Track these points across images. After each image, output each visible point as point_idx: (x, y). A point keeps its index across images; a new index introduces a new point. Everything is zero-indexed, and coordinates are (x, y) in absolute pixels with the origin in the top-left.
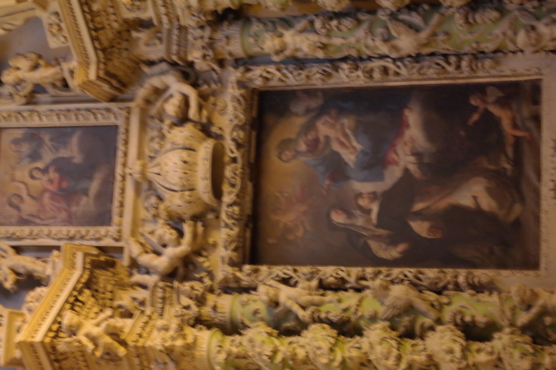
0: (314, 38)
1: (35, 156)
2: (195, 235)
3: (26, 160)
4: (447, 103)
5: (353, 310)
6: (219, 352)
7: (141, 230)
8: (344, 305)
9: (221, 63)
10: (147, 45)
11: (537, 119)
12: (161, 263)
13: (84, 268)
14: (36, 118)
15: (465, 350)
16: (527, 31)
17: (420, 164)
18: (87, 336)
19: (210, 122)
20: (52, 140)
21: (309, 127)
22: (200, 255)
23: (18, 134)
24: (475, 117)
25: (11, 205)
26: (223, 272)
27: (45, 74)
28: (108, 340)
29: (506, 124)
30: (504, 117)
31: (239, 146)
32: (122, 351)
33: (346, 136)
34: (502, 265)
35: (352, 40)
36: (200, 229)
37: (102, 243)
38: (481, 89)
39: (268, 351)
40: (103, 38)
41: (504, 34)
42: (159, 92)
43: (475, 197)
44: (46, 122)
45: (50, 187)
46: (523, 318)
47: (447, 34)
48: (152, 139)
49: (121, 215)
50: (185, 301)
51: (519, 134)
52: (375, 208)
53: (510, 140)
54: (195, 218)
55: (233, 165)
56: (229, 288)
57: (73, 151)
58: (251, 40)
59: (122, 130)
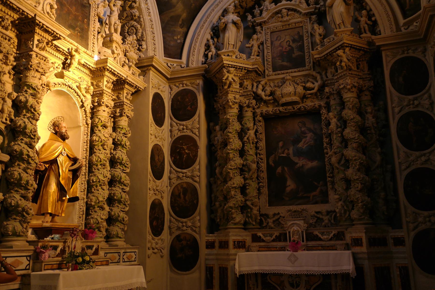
1: (294, 41)
2: (269, 100)
3: (292, 38)
5: (248, 153)
6: (230, 116)
7: (271, 82)
8: (249, 150)
10: (331, 72)
11: (316, 203)
12: (260, 92)
13: (253, 68)
14: (306, 39)
15: (235, 188)
16: (338, 198)
18: (228, 76)
19: (307, 98)
20: (300, 45)
21: (310, 130)
22: (264, 103)
23: (301, 34)
24: (316, 183)
25: (277, 38)
26: (258, 111)
27: (318, 39)
28: (228, 83)
29: (314, 193)
31: (299, 109)
32: (226, 87)
33: (307, 143)
34: (269, 196)
36: (271, 102)
38: (326, 185)
39: (230, 131)
40: (329, 57)
41: (339, 191)
42: (315, 79)
43: (290, 186)
44: (305, 41)
45: (284, 49)
46: (249, 203)
48: (301, 80)
49: (275, 75)
51: (311, 198)
55: (292, 108)
56: (255, 115)
57: (296, 53)
58: (334, 107)
59: (304, 68)
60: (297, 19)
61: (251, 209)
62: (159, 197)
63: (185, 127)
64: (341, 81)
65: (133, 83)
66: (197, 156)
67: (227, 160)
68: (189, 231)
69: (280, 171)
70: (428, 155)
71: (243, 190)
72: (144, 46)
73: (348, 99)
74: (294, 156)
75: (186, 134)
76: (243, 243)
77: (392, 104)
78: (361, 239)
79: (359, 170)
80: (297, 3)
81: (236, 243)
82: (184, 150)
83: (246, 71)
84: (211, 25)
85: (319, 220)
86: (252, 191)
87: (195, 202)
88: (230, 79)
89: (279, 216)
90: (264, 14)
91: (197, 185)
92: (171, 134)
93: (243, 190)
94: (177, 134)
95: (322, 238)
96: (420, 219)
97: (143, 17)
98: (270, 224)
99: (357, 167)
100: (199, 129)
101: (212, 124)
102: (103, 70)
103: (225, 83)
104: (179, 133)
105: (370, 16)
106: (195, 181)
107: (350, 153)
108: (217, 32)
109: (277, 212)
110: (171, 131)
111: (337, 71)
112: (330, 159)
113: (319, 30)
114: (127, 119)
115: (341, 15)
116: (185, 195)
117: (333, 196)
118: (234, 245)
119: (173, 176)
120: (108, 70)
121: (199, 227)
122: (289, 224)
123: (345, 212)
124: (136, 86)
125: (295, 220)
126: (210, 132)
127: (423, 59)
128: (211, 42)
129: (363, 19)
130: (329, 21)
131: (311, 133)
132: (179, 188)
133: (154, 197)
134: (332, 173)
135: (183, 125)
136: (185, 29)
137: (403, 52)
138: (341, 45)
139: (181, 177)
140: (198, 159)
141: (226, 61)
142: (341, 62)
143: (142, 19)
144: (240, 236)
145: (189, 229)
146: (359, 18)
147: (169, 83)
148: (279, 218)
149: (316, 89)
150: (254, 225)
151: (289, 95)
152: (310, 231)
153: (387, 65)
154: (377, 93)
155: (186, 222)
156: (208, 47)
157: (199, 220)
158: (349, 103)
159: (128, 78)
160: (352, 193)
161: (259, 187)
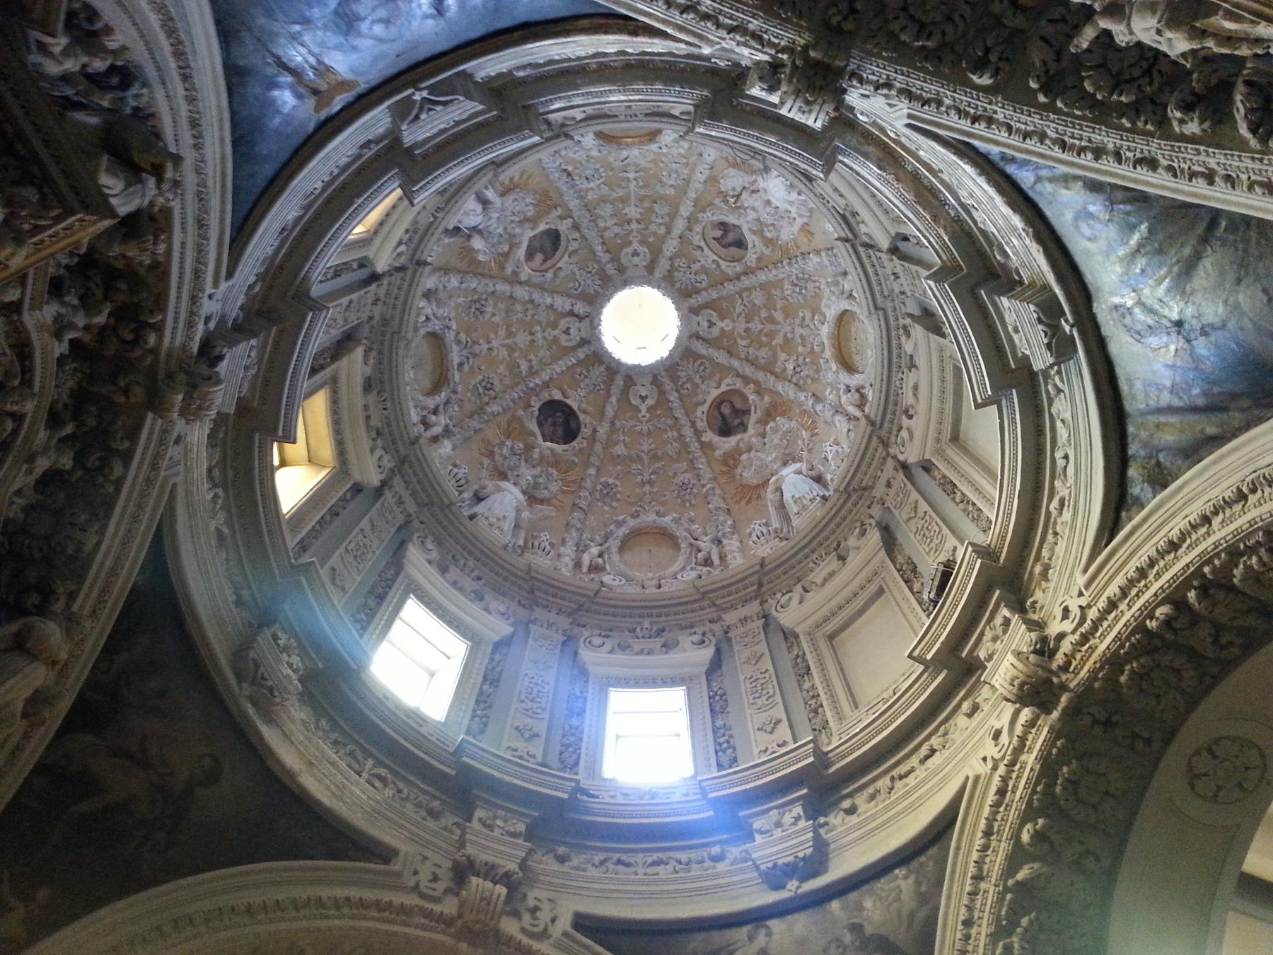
84: (150, 71)
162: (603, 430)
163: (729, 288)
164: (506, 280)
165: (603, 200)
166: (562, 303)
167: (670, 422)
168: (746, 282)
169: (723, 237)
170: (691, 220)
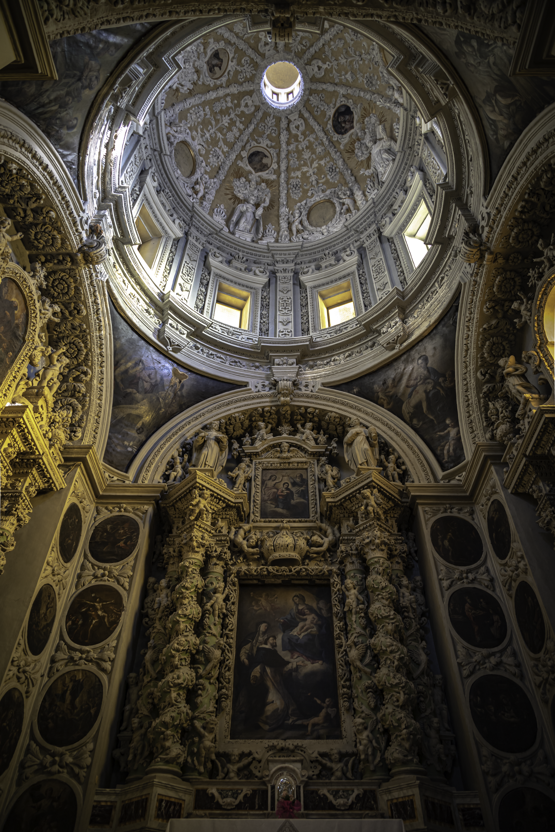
0: (354, 605)
1: (294, 484)
2: (253, 554)
4: (326, 685)
8: (212, 626)
9: (341, 562)
12: (240, 539)
16: (363, 724)
17: (291, 671)
18: (199, 501)
19: (311, 559)
21: (311, 610)
23: (304, 477)
24: (319, 702)
27: (330, 482)
29: (315, 720)
30: (319, 719)
31: (298, 572)
32: (192, 518)
33: (307, 630)
34: (233, 719)
35: (355, 626)
36: (256, 557)
37: (252, 515)
38: (335, 705)
41: (362, 712)
44: (310, 487)
46: (198, 724)
47: (361, 677)
50: (219, 550)
51: (309, 729)
52: (267, 647)
53: (305, 722)
54: (262, 554)
57: (296, 500)
60: (301, 458)
61: (201, 737)
62: (23, 689)
63: (107, 572)
64: (366, 534)
65: (47, 471)
66: (117, 624)
67: (170, 634)
68: (65, 776)
69: (258, 675)
70: (498, 655)
71: (192, 694)
72: (80, 435)
73: (376, 560)
74: (284, 649)
75: (107, 583)
76: (177, 808)
77: (438, 575)
78: (412, 801)
79: (398, 670)
80: (304, 438)
81: (164, 804)
82: (96, 610)
83: (224, 505)
84: (182, 439)
85: (325, 772)
86: (206, 701)
87: (92, 711)
88: (202, 506)
89: (250, 759)
90: (258, 444)
91: (104, 677)
92: (78, 582)
93: (192, 694)
94: (89, 581)
95: (334, 802)
96: (505, 768)
97: (90, 397)
98: (232, 775)
99: (396, 663)
100: (131, 578)
101: (152, 580)
102: (11, 424)
103: (192, 511)
104: (93, 582)
105: (399, 464)
106: (104, 670)
107: (382, 640)
108: (190, 450)
109: (246, 751)
110: (79, 577)
111: (356, 523)
112: (346, 654)
113: (331, 472)
114: (15, 522)
115: (365, 452)
116: (74, 694)
117: (349, 724)
118: (159, 808)
119: (61, 655)
120: (19, 426)
121: (89, 767)
122: (274, 770)
123: (374, 755)
124: (51, 478)
125: (284, 762)
126: (145, 593)
127: (471, 522)
128: (178, 460)
129: (391, 466)
130: (347, 460)
131: (313, 615)
132: (67, 680)
133: (14, 684)
134: (349, 680)
135: (105, 569)
136: (143, 437)
137: (445, 511)
138: (366, 485)
139: (76, 658)
140: (118, 630)
141: (202, 478)
142: (367, 505)
143: (88, 399)
144: (173, 789)
145: (65, 771)
146: (386, 463)
147: (97, 503)
148: (250, 763)
149: (326, 546)
150: (200, 774)
151: (286, 547)
152: (312, 788)
153: (426, 524)
154: (412, 563)
155: (62, 755)
156: (171, 466)
157: (92, 752)
158: (378, 565)
159: (44, 457)
160: (390, 710)
161: (220, 697)
162: (342, 91)
163: (242, 46)
164: (279, 177)
165: (225, 141)
166: (284, 137)
167: (326, 48)
168: (234, 40)
169: (217, 65)
170: (216, 88)
